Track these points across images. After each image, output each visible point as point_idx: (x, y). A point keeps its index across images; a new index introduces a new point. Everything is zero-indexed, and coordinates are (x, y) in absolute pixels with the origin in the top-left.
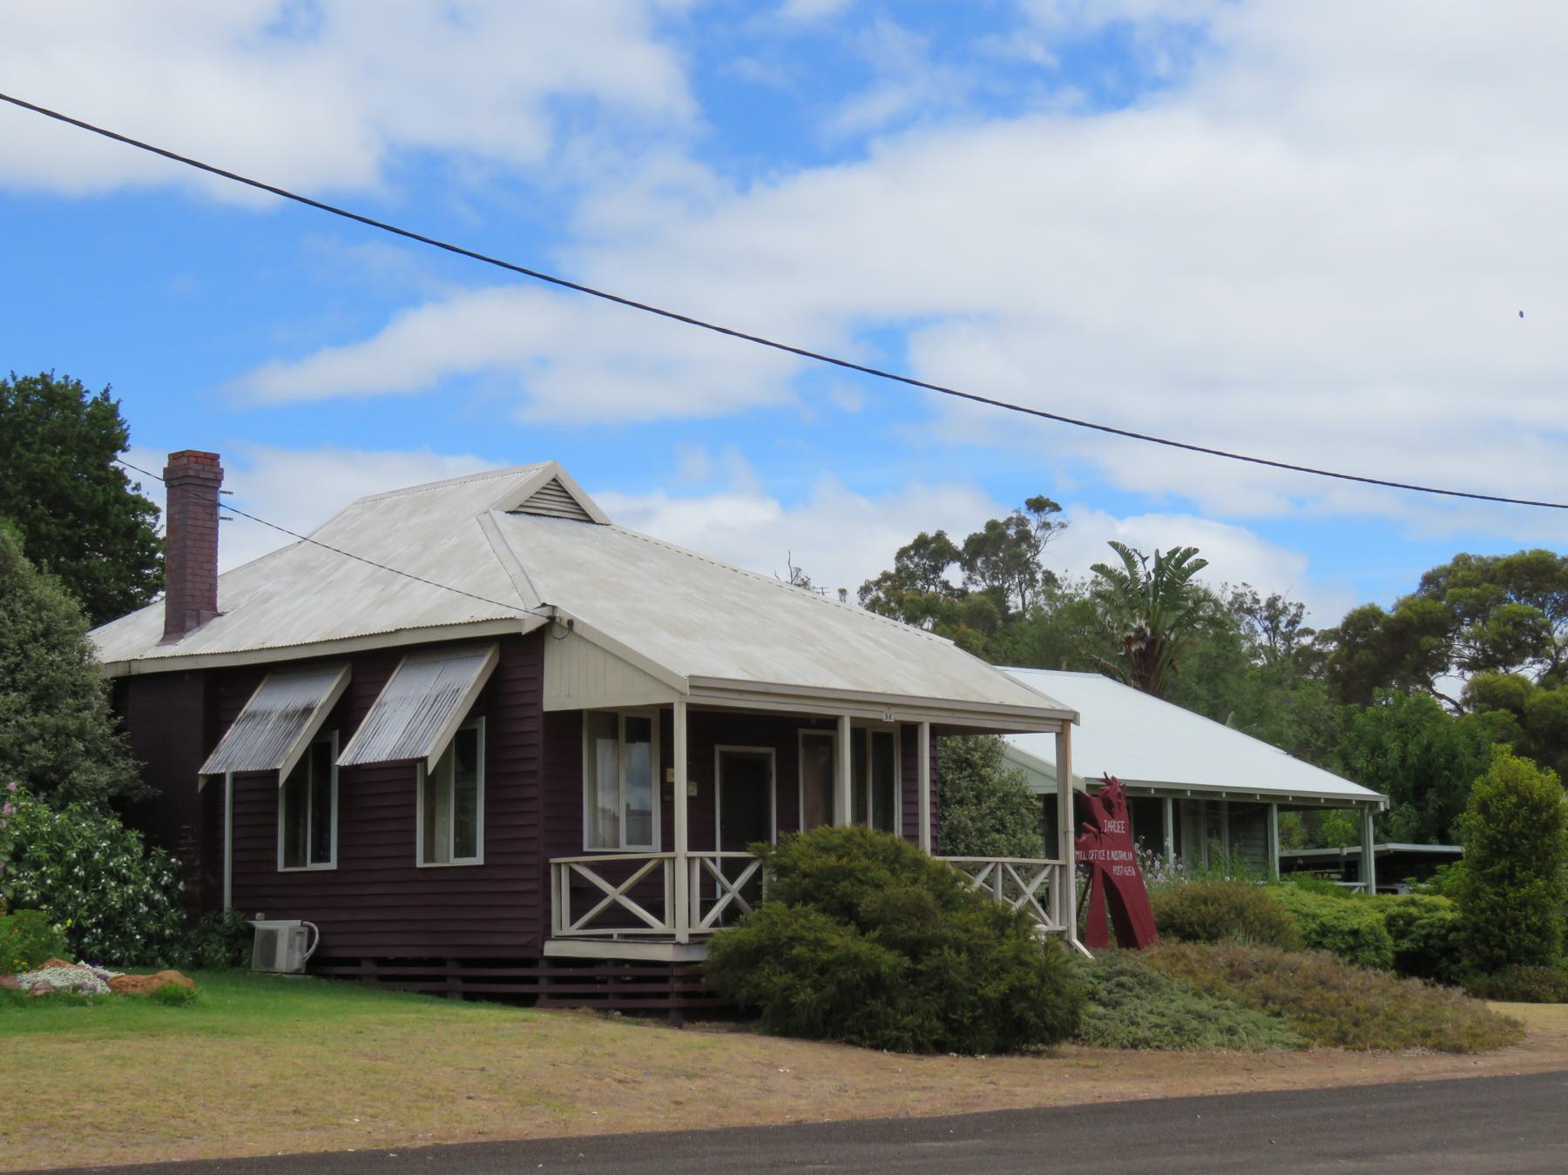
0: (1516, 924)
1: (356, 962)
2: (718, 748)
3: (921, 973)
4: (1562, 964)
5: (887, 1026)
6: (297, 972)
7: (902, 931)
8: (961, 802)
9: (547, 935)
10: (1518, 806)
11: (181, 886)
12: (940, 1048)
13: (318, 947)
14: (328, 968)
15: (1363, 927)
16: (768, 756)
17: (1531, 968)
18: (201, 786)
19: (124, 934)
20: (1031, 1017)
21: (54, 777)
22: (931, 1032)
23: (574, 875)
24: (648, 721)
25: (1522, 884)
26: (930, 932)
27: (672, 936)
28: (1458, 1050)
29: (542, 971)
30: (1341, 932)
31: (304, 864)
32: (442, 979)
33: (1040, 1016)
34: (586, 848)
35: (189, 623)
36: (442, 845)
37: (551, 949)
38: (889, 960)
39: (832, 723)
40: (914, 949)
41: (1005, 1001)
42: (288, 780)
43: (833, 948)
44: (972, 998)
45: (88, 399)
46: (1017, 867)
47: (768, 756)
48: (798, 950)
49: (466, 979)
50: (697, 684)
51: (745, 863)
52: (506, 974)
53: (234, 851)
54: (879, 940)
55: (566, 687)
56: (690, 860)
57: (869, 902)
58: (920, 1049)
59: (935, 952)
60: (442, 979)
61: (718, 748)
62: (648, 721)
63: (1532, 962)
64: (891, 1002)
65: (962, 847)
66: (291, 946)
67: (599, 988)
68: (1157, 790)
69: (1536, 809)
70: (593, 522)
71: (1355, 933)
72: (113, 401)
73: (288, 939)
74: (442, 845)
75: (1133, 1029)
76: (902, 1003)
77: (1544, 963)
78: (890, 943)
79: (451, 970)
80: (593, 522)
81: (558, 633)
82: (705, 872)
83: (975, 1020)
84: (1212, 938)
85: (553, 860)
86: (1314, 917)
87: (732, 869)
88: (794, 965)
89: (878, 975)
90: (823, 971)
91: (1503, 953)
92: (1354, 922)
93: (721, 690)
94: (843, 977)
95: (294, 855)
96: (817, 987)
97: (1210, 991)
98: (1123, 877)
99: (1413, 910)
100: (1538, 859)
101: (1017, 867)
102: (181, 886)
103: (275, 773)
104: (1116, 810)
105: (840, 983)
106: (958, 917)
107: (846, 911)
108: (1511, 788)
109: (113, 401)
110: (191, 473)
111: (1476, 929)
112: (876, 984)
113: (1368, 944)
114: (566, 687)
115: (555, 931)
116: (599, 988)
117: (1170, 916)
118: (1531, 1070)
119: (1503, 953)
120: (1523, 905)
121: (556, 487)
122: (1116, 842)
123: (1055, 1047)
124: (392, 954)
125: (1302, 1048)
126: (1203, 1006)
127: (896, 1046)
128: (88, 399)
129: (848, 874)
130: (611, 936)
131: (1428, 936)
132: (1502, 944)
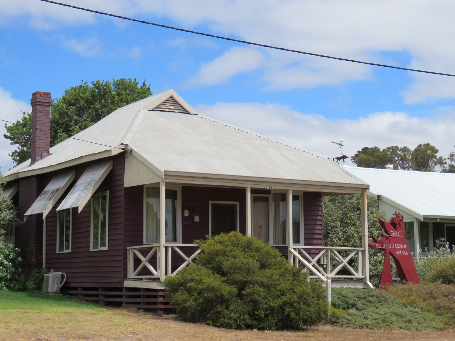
1: (76, 289)
2: (211, 202)
5: (224, 317)
6: (56, 293)
7: (239, 277)
9: (125, 277)
12: (249, 327)
13: (65, 283)
16: (236, 205)
18: (25, 220)
20: (293, 315)
22: (244, 320)
23: (135, 254)
24: (176, 191)
26: (249, 278)
27: (159, 279)
29: (124, 293)
31: (63, 251)
32: (97, 295)
33: (297, 315)
34: (144, 243)
35: (37, 158)
36: (99, 243)
37: (127, 284)
38: (227, 290)
39: (242, 191)
41: (282, 308)
42: (47, 217)
45: (139, 86)
46: (340, 252)
47: (236, 205)
48: (193, 284)
49: (107, 296)
50: (168, 174)
51: (194, 249)
55: (132, 178)
56: (166, 248)
57: (226, 265)
58: (239, 328)
60: (97, 295)
61: (211, 202)
62: (176, 191)
64: (227, 308)
66: (53, 282)
67: (138, 300)
68: (441, 219)
70: (189, 114)
72: (147, 86)
73: (53, 280)
74: (99, 243)
75: (365, 320)
76: (232, 307)
78: (230, 282)
79: (79, 291)
80: (189, 114)
81: (128, 155)
82: (174, 252)
83: (266, 316)
85: (128, 248)
87: (189, 251)
88: (189, 291)
89: (222, 295)
93: (182, 176)
94: (206, 295)
95: (61, 248)
96: (196, 300)
97: (411, 304)
98: (401, 255)
101: (340, 252)
102: (20, 259)
104: (398, 227)
105: (205, 298)
106: (268, 272)
107: (219, 270)
109: (147, 86)
110: (38, 100)
112: (223, 300)
114: (132, 178)
115: (129, 277)
117: (441, 272)
121: (172, 99)
122: (397, 240)
123: (316, 328)
124: (86, 285)
125: (441, 329)
126: (404, 311)
127: (228, 326)
128: (139, 86)
129: (224, 254)
130: (142, 279)
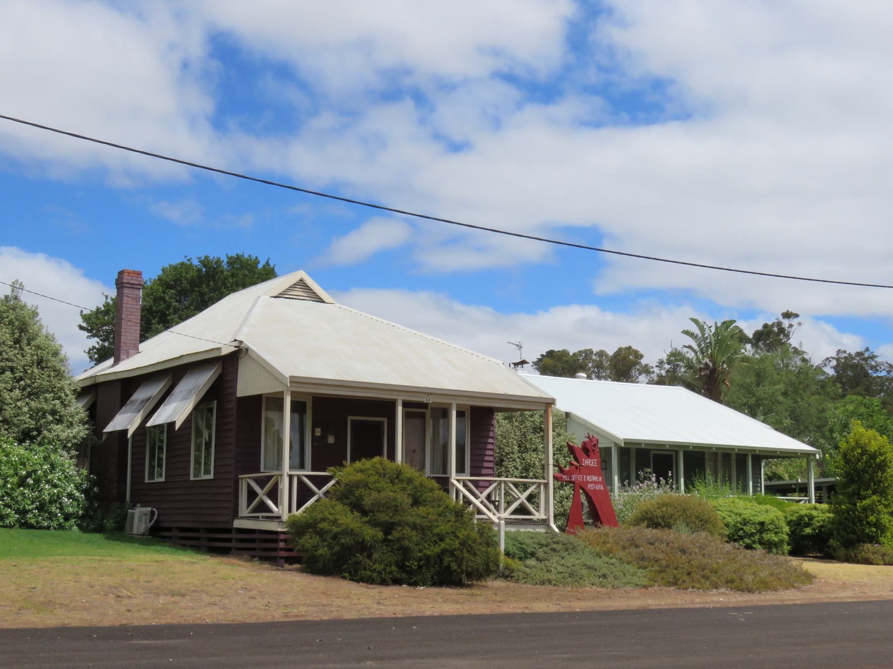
0: (860, 521)
1: (169, 529)
2: (350, 418)
3: (390, 541)
4: (888, 545)
5: (365, 569)
6: (143, 534)
7: (383, 517)
8: (535, 450)
9: (235, 514)
10: (862, 454)
11: (95, 489)
12: (397, 582)
13: (156, 522)
14: (159, 534)
15: (767, 521)
16: (382, 422)
17: (869, 545)
18: (104, 438)
19: (50, 513)
20: (454, 566)
21: (35, 433)
22: (391, 572)
23: (249, 485)
24: (305, 403)
25: (864, 498)
26: (397, 518)
27: (279, 517)
28: (750, 591)
29: (234, 536)
30: (754, 523)
31: (153, 479)
32: (197, 539)
33: (460, 566)
34: (262, 470)
35: (122, 357)
36: (201, 470)
37: (238, 524)
38: (371, 533)
39: (392, 404)
40: (387, 528)
41: (440, 557)
42: (134, 435)
43: (341, 524)
44: (419, 554)
45: (260, 266)
46: (516, 485)
47: (382, 422)
48: (324, 525)
49: (211, 540)
50: (295, 381)
51: (327, 479)
52: (215, 537)
53: (144, 471)
54: (368, 522)
55: (247, 385)
56: (291, 477)
57: (367, 501)
58: (384, 583)
59: (399, 528)
60: (197, 539)
61: (350, 418)
62: (305, 403)
63: (871, 542)
64: (369, 556)
65: (531, 474)
66: (140, 521)
67: (252, 545)
68: (646, 444)
69: (873, 456)
70: (324, 302)
71: (762, 524)
72: (272, 266)
73: (140, 517)
74: (201, 470)
75: (548, 574)
76: (375, 556)
77: (878, 542)
78: (374, 524)
79: (174, 533)
80: (324, 302)
81: (243, 355)
82: (301, 483)
83: (420, 567)
84: (669, 526)
85: (240, 476)
86: (740, 515)
87: (320, 482)
88: (321, 533)
89: (363, 541)
90: (335, 537)
91: (854, 536)
92: (761, 518)
93: (313, 384)
94: (343, 541)
95: (151, 476)
96: (330, 547)
97: (607, 553)
98: (595, 491)
99: (814, 513)
100: (875, 485)
101: (516, 485)
102: (95, 489)
103: (126, 431)
104: (591, 453)
105: (343, 544)
106: (422, 510)
107: (357, 506)
108: (858, 444)
109: (272, 266)
110: (125, 281)
111: (841, 523)
112: (364, 547)
113: (769, 530)
114: (247, 385)
115: (241, 514)
116: (252, 545)
117: (646, 513)
118: (814, 601)
119: (854, 536)
120: (865, 509)
121: (302, 284)
122: (590, 471)
123: (484, 583)
124: (184, 525)
125: (645, 587)
126: (598, 562)
127: (370, 581)
128: (260, 266)
129: (366, 485)
130: (258, 517)
131: (822, 526)
132: (854, 532)
